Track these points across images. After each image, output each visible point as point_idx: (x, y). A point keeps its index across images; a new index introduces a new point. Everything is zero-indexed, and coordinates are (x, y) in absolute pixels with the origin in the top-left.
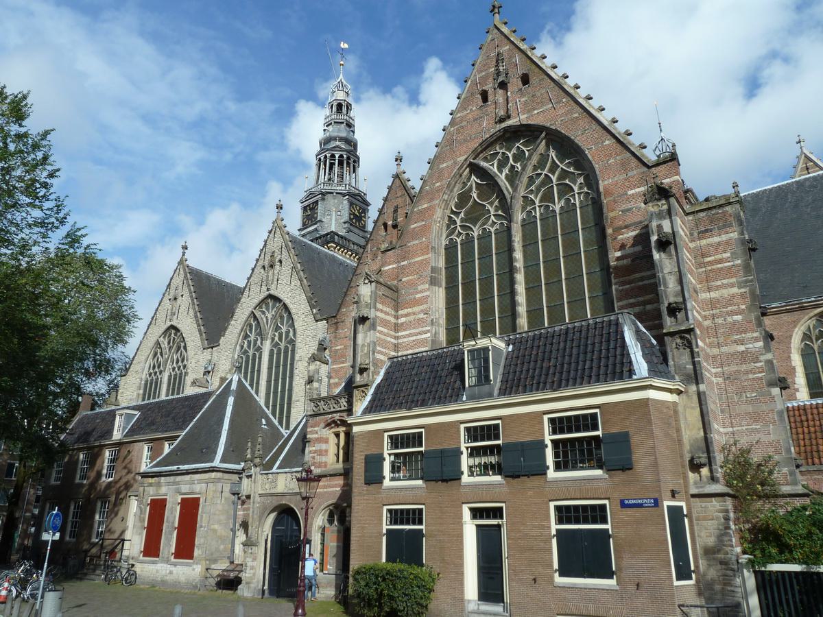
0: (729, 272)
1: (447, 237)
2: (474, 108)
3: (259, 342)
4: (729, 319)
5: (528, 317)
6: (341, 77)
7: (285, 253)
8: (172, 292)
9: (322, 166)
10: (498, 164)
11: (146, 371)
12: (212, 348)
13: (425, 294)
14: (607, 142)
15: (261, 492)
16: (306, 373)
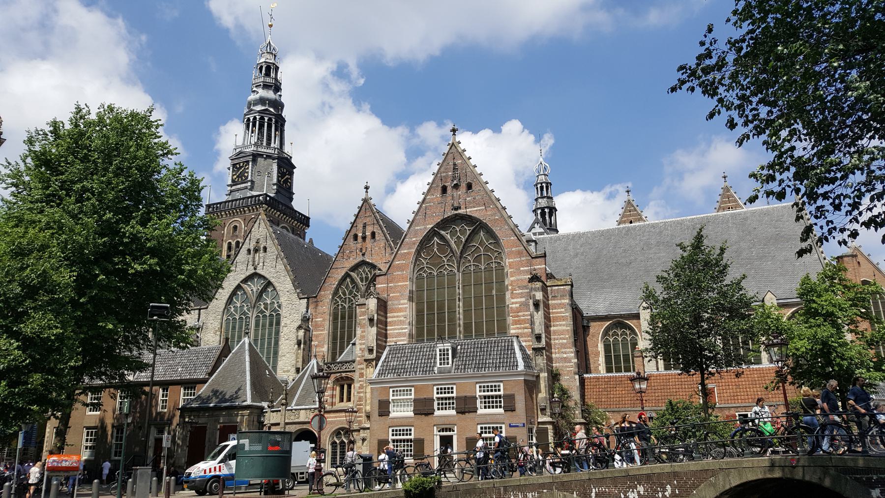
3: (245, 308)
5: (464, 326)
7: (269, 242)
12: (200, 310)
13: (405, 306)
14: (512, 238)
15: (287, 421)
16: (294, 336)
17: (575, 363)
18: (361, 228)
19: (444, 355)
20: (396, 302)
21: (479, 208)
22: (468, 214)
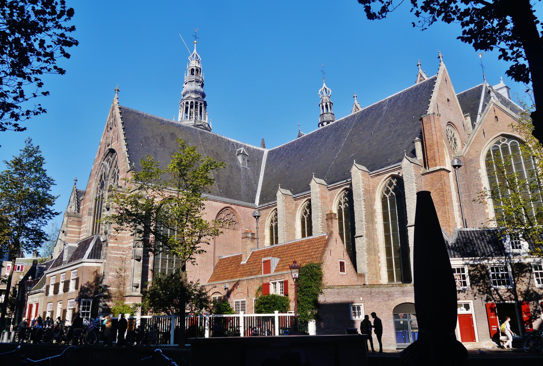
6: (195, 51)
22: (112, 148)
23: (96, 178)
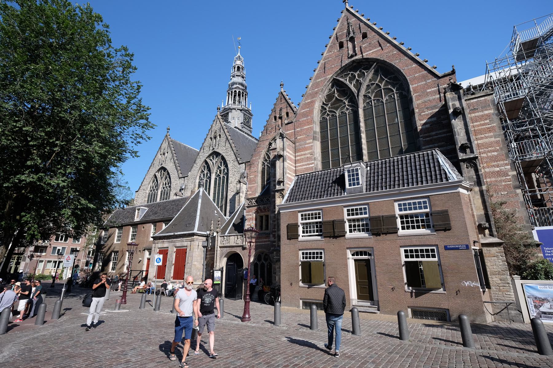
0: (490, 130)
1: (321, 116)
2: (336, 51)
4: (489, 154)
6: (239, 53)
8: (162, 151)
9: (230, 96)
10: (349, 79)
11: (149, 188)
12: (184, 177)
13: (311, 145)
17: (513, 176)
18: (279, 112)
19: (353, 175)
20: (302, 143)
21: (375, 50)
22: (365, 57)
23: (320, 96)
